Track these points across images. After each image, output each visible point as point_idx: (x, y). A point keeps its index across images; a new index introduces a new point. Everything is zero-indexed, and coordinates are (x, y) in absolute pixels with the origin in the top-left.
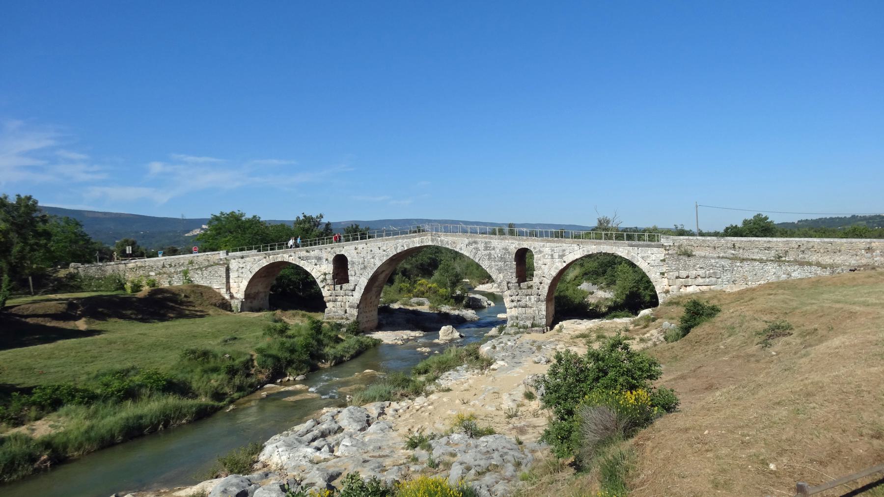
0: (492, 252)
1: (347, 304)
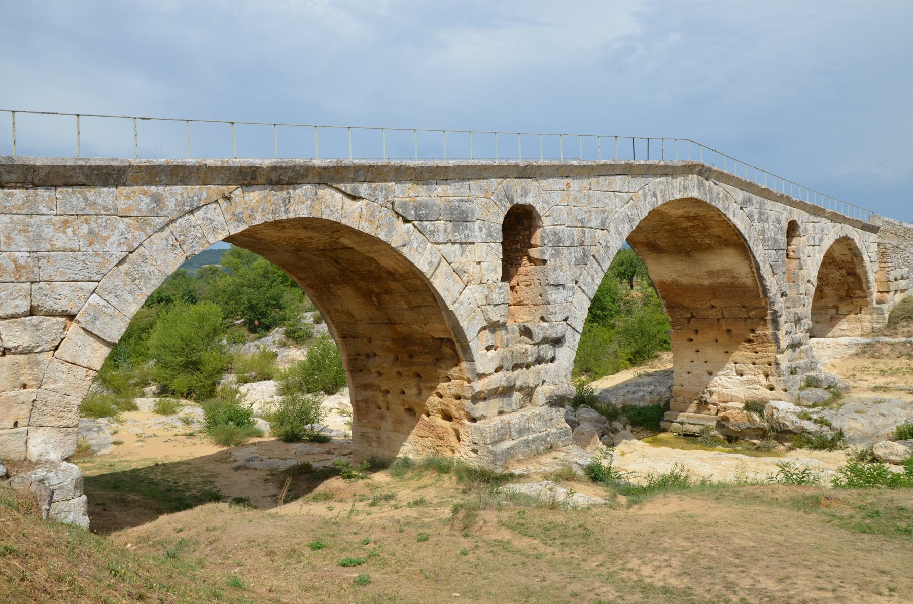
0: (766, 225)
1: (542, 393)
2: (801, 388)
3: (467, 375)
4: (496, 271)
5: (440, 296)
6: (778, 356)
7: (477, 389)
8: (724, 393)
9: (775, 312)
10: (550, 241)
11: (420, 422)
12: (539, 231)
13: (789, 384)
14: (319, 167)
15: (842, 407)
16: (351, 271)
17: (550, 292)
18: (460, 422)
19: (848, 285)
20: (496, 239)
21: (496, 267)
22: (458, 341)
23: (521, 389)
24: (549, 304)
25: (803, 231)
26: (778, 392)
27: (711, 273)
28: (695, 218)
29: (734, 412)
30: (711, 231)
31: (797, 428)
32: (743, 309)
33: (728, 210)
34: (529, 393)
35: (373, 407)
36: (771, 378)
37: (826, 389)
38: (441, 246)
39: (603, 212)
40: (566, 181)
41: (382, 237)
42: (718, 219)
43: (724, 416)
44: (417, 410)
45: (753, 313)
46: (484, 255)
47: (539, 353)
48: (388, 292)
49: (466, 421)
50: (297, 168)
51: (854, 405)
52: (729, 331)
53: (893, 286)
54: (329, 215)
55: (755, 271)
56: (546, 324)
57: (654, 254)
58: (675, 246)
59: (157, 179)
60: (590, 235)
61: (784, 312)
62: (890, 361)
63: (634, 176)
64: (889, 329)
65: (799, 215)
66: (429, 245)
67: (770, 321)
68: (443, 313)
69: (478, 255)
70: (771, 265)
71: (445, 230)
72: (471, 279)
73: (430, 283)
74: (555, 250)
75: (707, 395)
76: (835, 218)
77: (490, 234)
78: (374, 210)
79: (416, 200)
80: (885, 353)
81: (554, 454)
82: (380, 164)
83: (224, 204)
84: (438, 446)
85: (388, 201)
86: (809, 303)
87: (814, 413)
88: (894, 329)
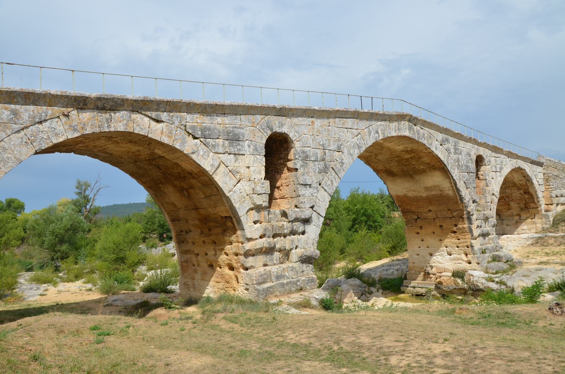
0: (460, 157)
1: (295, 254)
2: (489, 262)
3: (241, 239)
4: (260, 173)
5: (219, 186)
6: (472, 241)
7: (247, 248)
8: (440, 267)
9: (469, 212)
10: (300, 157)
11: (216, 272)
12: (293, 150)
13: (480, 259)
14: (131, 100)
15: (515, 273)
16: (169, 174)
17: (300, 189)
18: (238, 270)
19: (525, 201)
20: (260, 153)
21: (260, 171)
22: (234, 217)
23: (280, 251)
24: (300, 196)
25: (487, 162)
26: (474, 265)
27: (427, 189)
28: (412, 151)
29: (445, 278)
30: (423, 160)
31: (485, 287)
32: (449, 211)
33: (431, 145)
34: (286, 254)
35: (190, 265)
36: (469, 256)
37: (505, 262)
38: (220, 155)
39: (339, 141)
40: (311, 119)
41: (177, 146)
42: (426, 151)
43: (439, 281)
44: (214, 265)
45: (455, 213)
46: (252, 163)
47: (292, 227)
48: (192, 187)
49: (242, 270)
50: (115, 100)
51: (522, 272)
52: (441, 226)
53: (555, 201)
54: (139, 131)
55: (454, 186)
56: (297, 210)
57: (390, 178)
58: (403, 171)
59: (15, 100)
60: (329, 155)
61: (475, 213)
62: (553, 248)
63: (361, 119)
64: (553, 228)
65: (483, 151)
66: (212, 154)
67: (466, 219)
68: (224, 199)
69: (247, 162)
70: (464, 182)
71: (223, 145)
72: (242, 177)
73: (213, 178)
74: (304, 163)
75: (429, 269)
76: (510, 155)
77: (256, 149)
78: (172, 130)
79: (202, 125)
80: (551, 243)
81: (302, 293)
82: (175, 100)
83: (64, 119)
84: (226, 288)
85: (182, 125)
86: (494, 208)
87: (496, 277)
88: (556, 228)
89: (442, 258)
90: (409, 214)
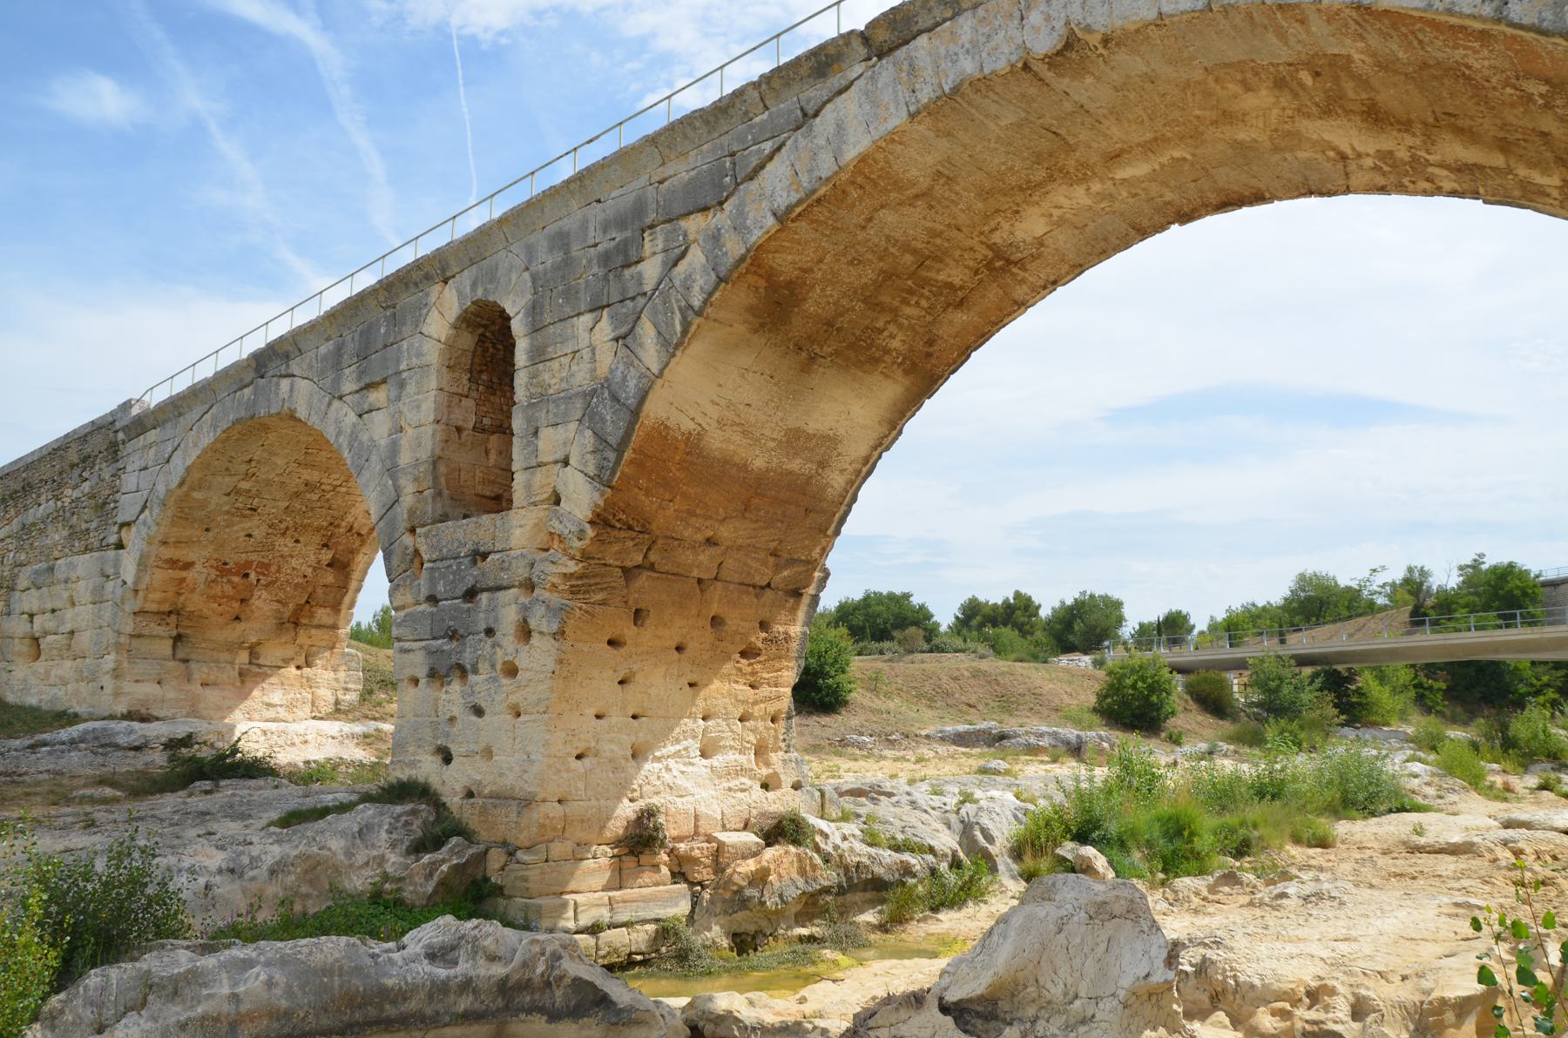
32: (772, 560)
36: (776, 758)
45: (786, 573)
89: (684, 769)
90: (623, 534)
